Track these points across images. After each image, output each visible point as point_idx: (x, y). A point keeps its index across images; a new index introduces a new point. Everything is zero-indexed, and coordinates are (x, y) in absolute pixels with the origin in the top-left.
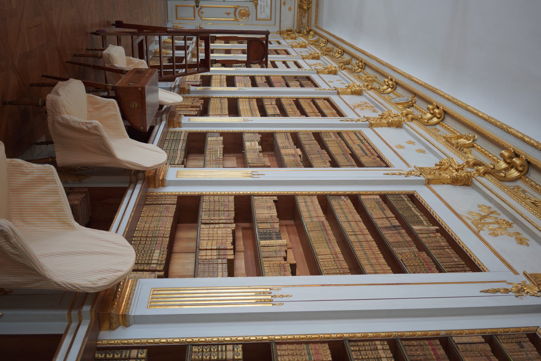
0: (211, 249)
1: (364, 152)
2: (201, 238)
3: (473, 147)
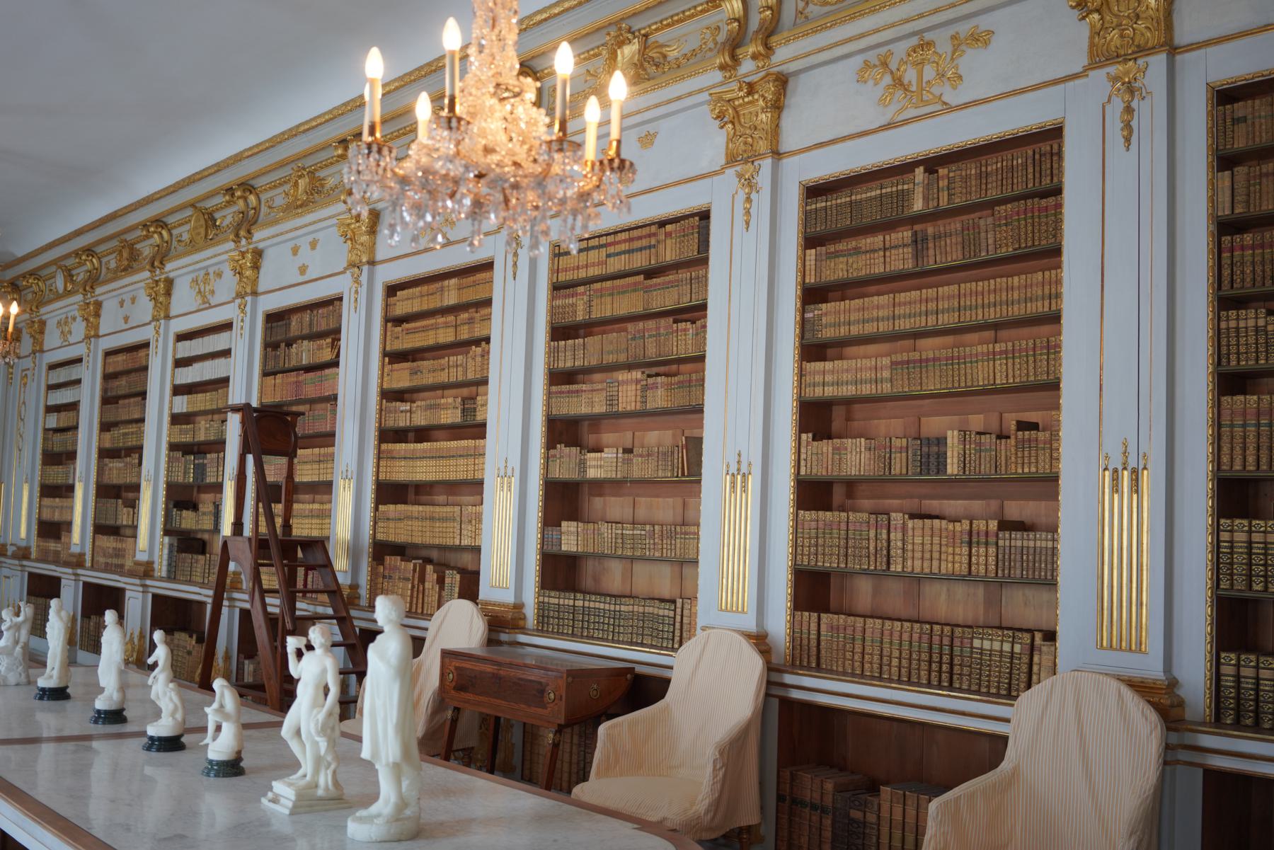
1: (641, 249)
2: (935, 570)
3: (646, 36)
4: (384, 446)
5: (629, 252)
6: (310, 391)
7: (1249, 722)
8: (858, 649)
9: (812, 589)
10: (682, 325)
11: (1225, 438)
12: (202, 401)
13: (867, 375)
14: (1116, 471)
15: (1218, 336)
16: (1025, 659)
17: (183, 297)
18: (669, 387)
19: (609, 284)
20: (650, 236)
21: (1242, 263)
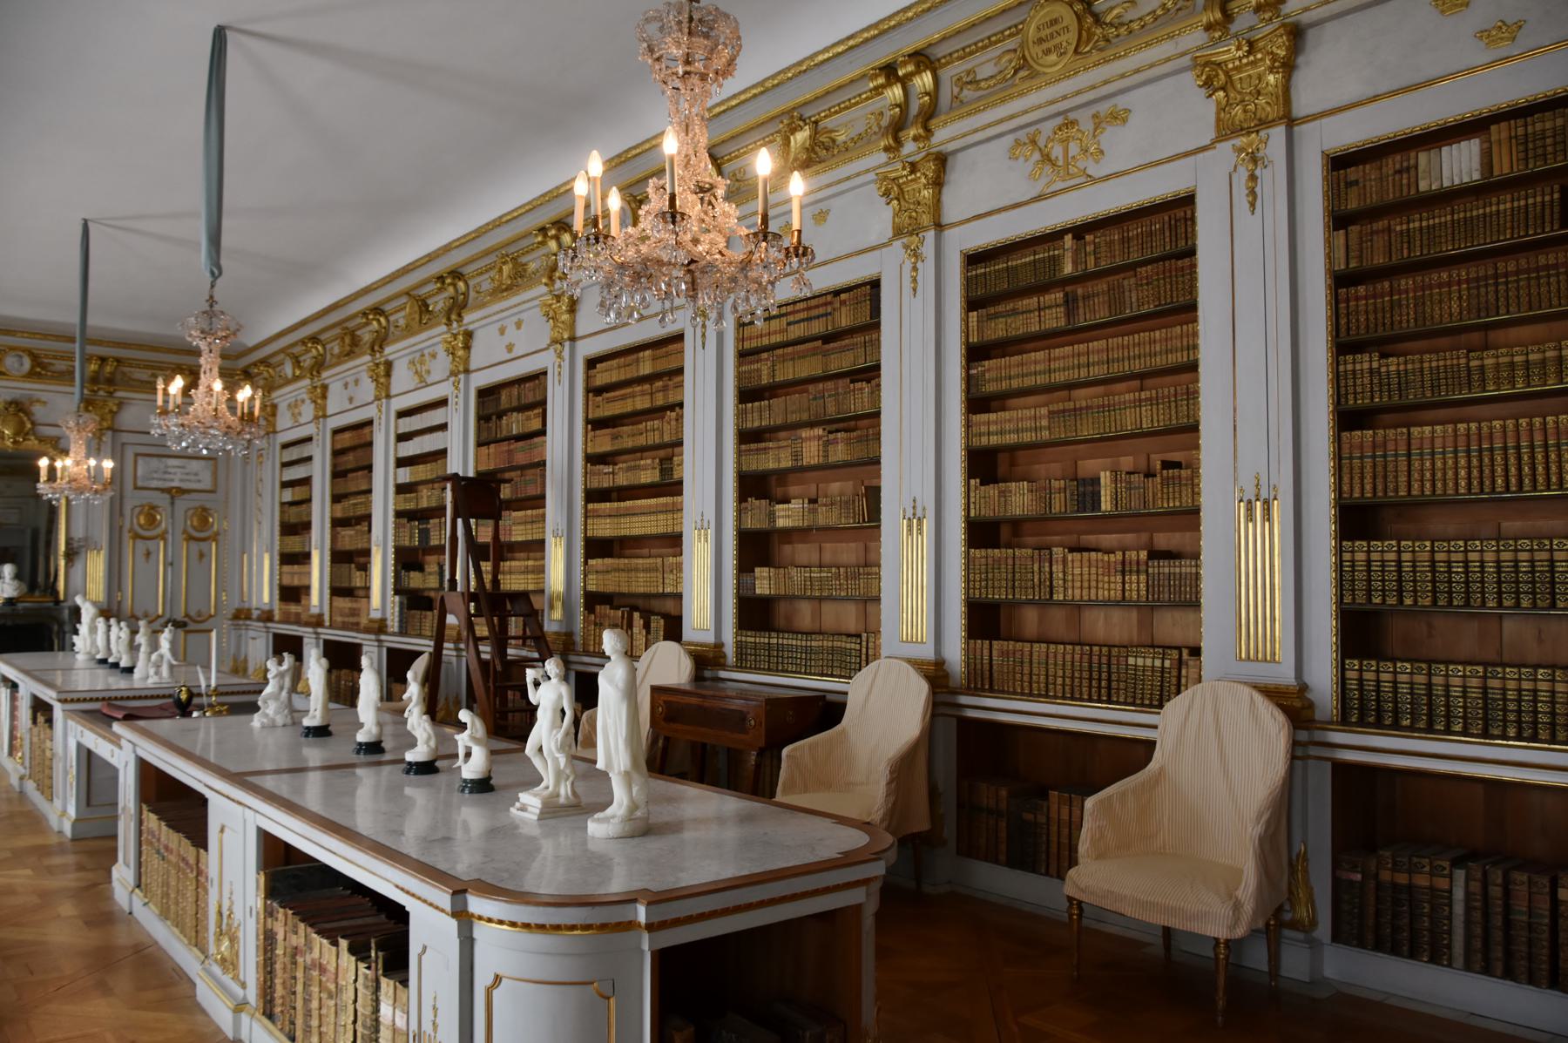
0: (1124, 583)
2: (1093, 597)
3: (816, 122)
4: (590, 506)
5: (809, 319)
6: (521, 458)
7: (1371, 719)
8: (1026, 670)
9: (985, 619)
10: (858, 385)
11: (1345, 470)
12: (423, 472)
13: (1027, 424)
14: (1249, 502)
15: (1339, 381)
16: (1174, 673)
17: (402, 377)
18: (848, 442)
19: (790, 349)
20: (826, 304)
21: (1357, 312)
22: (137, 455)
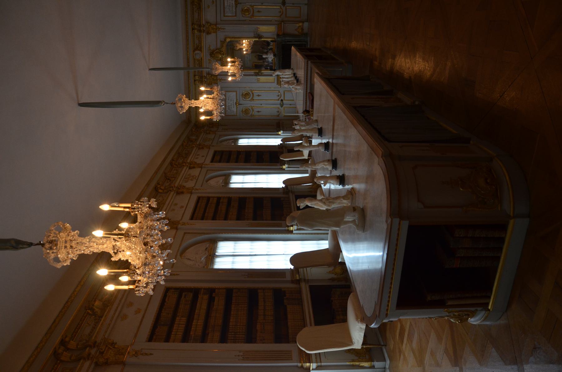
22: (224, 16)
